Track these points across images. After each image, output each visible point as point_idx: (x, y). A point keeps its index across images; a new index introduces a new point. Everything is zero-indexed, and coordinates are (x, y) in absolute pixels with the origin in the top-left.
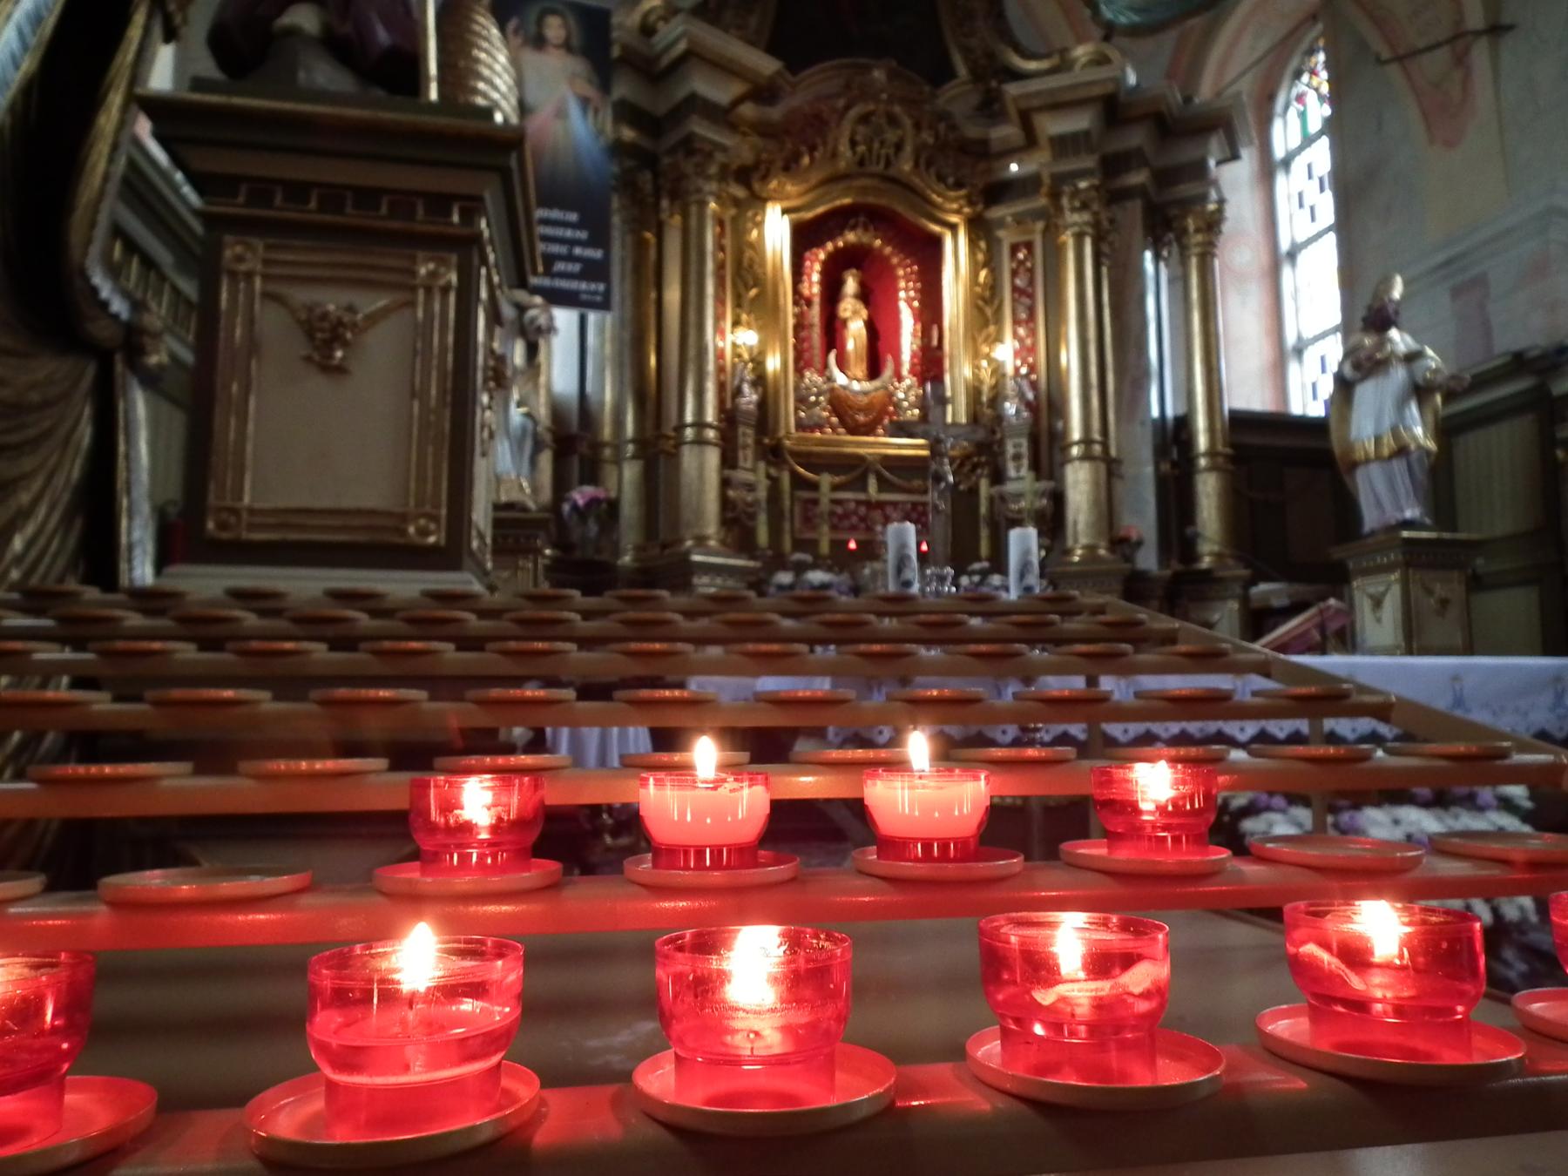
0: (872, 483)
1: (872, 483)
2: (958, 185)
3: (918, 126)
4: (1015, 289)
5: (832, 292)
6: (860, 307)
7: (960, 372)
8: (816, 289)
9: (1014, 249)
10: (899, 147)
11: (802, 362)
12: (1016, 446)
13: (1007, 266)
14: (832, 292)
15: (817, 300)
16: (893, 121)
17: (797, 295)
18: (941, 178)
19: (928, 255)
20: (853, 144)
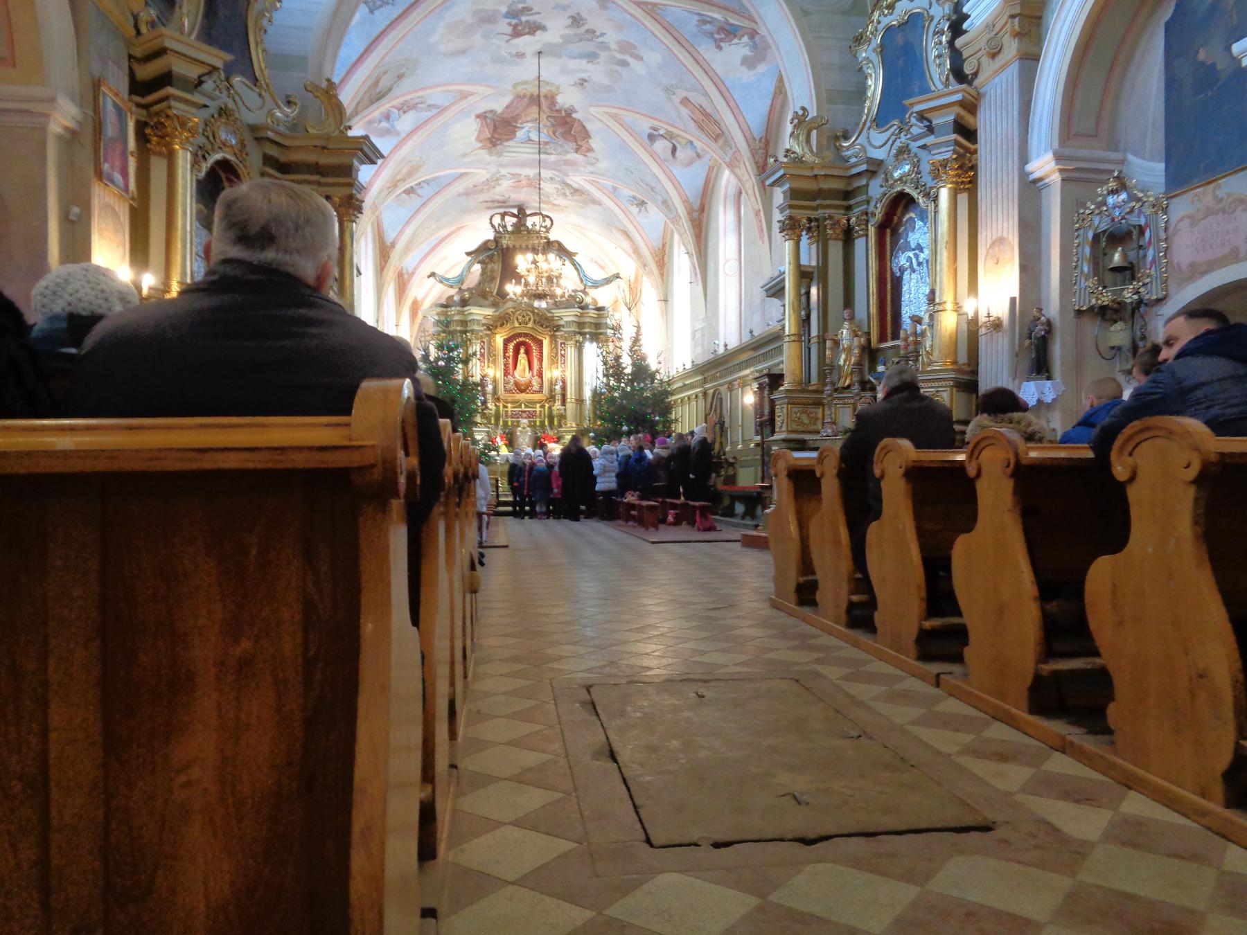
0: (523, 405)
1: (523, 405)
2: (547, 327)
3: (534, 315)
4: (562, 355)
5: (516, 352)
6: (525, 355)
7: (547, 375)
8: (511, 354)
9: (561, 344)
10: (530, 319)
11: (506, 374)
12: (558, 397)
13: (559, 348)
14: (516, 352)
15: (511, 358)
16: (528, 315)
17: (505, 357)
18: (542, 326)
19: (540, 344)
20: (518, 320)
